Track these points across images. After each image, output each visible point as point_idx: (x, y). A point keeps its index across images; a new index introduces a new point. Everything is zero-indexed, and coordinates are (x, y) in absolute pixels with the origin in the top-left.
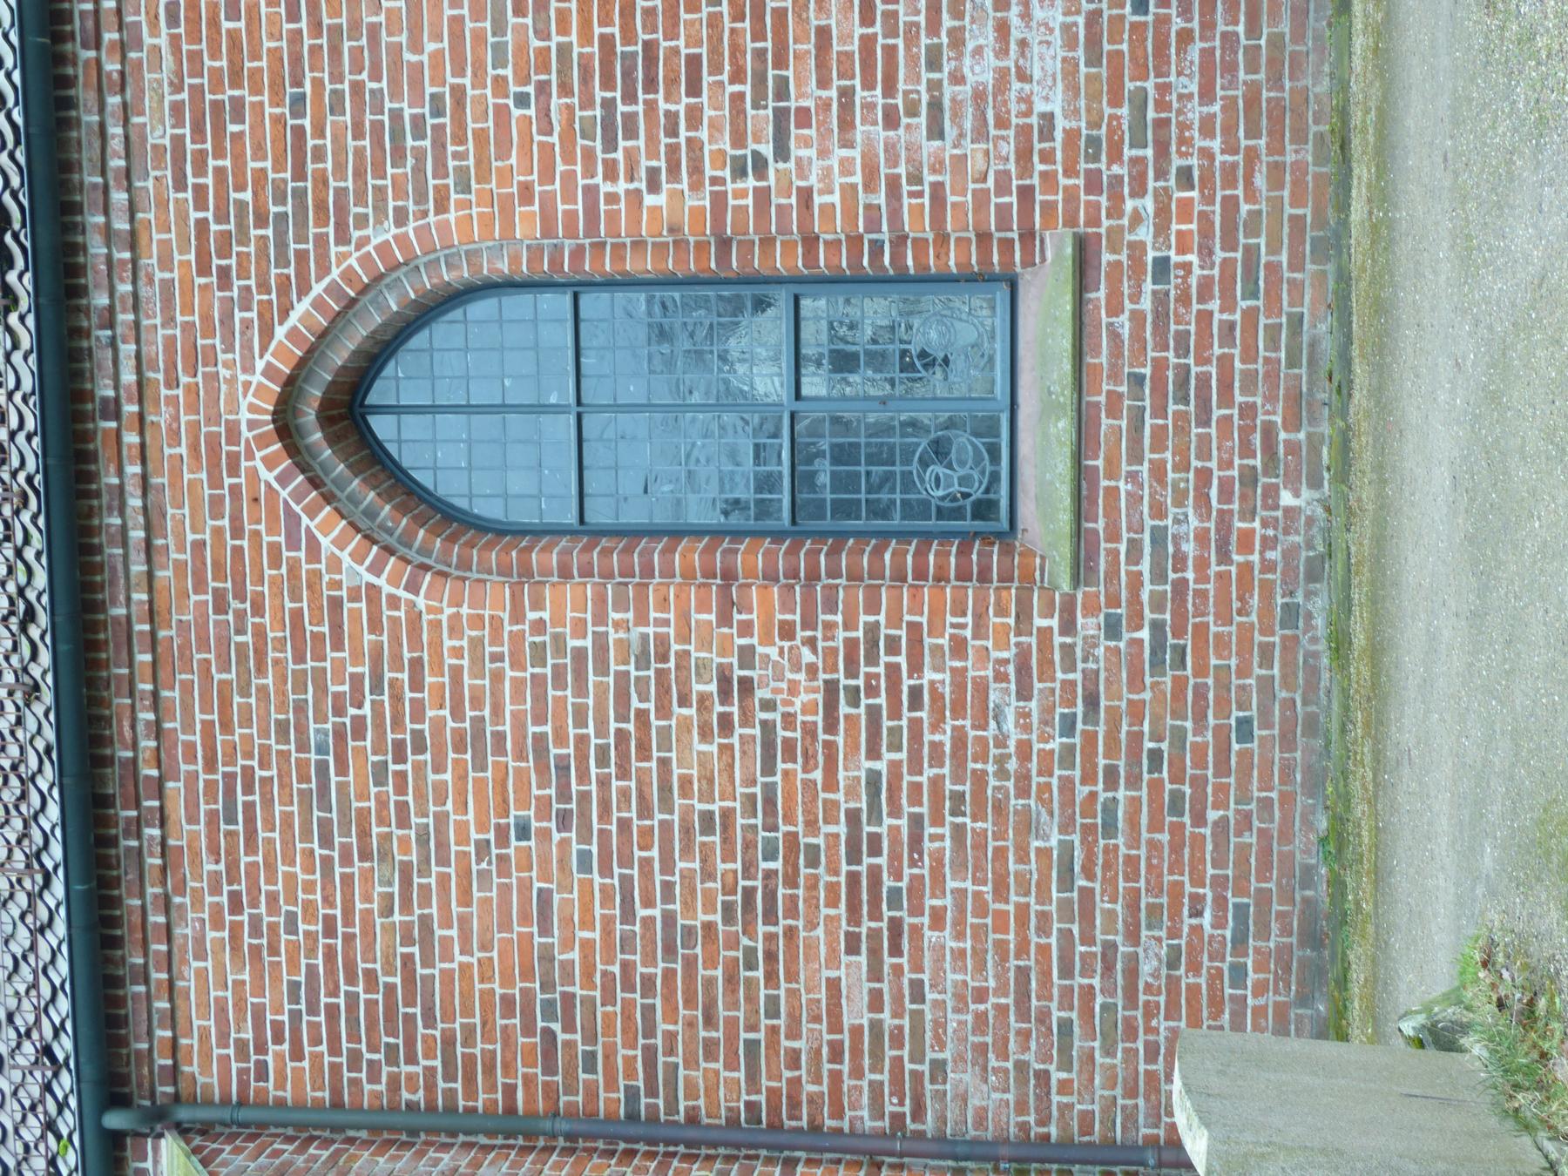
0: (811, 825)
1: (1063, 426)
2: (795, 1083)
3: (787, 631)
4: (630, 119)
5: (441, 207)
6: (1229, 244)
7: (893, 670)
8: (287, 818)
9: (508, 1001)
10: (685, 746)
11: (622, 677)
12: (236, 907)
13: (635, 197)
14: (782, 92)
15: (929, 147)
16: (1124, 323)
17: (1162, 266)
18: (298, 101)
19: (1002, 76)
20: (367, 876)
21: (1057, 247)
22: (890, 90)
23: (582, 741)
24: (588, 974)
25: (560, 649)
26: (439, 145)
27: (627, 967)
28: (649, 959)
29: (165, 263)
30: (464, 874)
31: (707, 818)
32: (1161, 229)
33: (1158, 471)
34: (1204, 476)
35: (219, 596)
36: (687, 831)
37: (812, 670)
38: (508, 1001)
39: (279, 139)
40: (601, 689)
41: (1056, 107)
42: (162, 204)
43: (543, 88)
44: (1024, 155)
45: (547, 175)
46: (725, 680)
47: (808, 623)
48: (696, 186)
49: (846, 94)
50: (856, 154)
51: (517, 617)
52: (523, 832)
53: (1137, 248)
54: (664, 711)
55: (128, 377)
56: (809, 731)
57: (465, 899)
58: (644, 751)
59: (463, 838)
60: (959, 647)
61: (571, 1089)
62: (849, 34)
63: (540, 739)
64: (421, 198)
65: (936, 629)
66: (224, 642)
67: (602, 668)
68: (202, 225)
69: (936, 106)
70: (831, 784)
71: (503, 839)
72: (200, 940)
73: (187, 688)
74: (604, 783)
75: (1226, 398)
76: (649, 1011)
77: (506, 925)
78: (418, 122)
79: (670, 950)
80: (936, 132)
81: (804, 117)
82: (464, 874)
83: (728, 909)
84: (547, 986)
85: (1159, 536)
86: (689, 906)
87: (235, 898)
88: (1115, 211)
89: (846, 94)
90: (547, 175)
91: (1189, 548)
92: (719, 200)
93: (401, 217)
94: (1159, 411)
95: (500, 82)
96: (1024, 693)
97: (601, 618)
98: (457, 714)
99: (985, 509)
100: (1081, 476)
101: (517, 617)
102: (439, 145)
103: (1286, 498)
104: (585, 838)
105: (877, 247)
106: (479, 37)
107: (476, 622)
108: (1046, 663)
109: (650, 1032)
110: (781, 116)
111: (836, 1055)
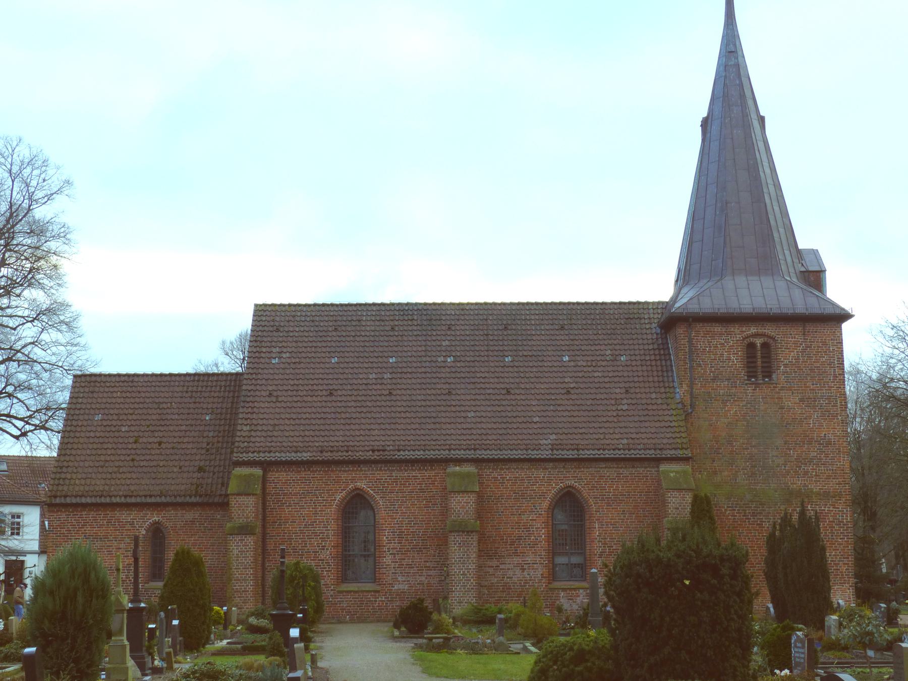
0: (305, 558)
1: (357, 589)
2: (271, 555)
4: (395, 535)
5: (385, 510)
6: (379, 609)
7: (326, 568)
8: (305, 488)
9: (281, 517)
10: (316, 541)
11: (324, 533)
12: (293, 480)
13: (385, 535)
14: (398, 554)
15: (391, 572)
16: (369, 596)
17: (376, 601)
18: (397, 492)
19: (399, 581)
20: (297, 498)
21: (378, 588)
22: (398, 567)
23: (316, 527)
24: (286, 528)
25: (328, 525)
26: (392, 510)
27: (286, 533)
28: (287, 536)
29: (378, 474)
30: (298, 511)
31: (306, 544)
32: (380, 601)
33: (351, 601)
34: (350, 607)
35: (335, 480)
36: (305, 541)
37: (326, 558)
38: (281, 517)
39: (393, 490)
40: (323, 530)
41: (395, 588)
42: (385, 474)
43: (399, 524)
44: (390, 584)
45: (388, 524)
47: (332, 557)
48: (387, 543)
49: (397, 562)
50: (390, 563)
51: (332, 519)
52: (304, 519)
53: (378, 598)
54: (320, 538)
55: (363, 469)
56: (318, 557)
57: (295, 511)
58: (315, 536)
59: (303, 511)
60: (329, 576)
61: (270, 525)
63: (316, 522)
64: (386, 508)
65: (331, 574)
66: (329, 480)
67: (326, 530)
68: (382, 479)
69: (396, 573)
70: (311, 560)
71: (303, 517)
72: (288, 475)
73: (322, 474)
74: (311, 530)
75: (360, 609)
76: (280, 536)
77: (291, 517)
78: (395, 508)
79: (288, 539)
80: (393, 573)
81: (395, 557)
82: (298, 511)
83: (294, 547)
84: (283, 522)
85: (343, 601)
86: (295, 541)
87: (294, 480)
88: (383, 595)
89: (397, 562)
90: (388, 524)
91: (342, 605)
92: (385, 546)
93: (383, 505)
94: (359, 601)
95: (399, 518)
97: (332, 530)
98: (319, 511)
99: (346, 579)
100: (351, 592)
101: (332, 519)
102: (392, 510)
103: (348, 617)
104: (304, 528)
105: (379, 565)
106: (405, 516)
107: (331, 514)
108: (327, 587)
109: (278, 536)
110: (395, 554)
111: (275, 561)
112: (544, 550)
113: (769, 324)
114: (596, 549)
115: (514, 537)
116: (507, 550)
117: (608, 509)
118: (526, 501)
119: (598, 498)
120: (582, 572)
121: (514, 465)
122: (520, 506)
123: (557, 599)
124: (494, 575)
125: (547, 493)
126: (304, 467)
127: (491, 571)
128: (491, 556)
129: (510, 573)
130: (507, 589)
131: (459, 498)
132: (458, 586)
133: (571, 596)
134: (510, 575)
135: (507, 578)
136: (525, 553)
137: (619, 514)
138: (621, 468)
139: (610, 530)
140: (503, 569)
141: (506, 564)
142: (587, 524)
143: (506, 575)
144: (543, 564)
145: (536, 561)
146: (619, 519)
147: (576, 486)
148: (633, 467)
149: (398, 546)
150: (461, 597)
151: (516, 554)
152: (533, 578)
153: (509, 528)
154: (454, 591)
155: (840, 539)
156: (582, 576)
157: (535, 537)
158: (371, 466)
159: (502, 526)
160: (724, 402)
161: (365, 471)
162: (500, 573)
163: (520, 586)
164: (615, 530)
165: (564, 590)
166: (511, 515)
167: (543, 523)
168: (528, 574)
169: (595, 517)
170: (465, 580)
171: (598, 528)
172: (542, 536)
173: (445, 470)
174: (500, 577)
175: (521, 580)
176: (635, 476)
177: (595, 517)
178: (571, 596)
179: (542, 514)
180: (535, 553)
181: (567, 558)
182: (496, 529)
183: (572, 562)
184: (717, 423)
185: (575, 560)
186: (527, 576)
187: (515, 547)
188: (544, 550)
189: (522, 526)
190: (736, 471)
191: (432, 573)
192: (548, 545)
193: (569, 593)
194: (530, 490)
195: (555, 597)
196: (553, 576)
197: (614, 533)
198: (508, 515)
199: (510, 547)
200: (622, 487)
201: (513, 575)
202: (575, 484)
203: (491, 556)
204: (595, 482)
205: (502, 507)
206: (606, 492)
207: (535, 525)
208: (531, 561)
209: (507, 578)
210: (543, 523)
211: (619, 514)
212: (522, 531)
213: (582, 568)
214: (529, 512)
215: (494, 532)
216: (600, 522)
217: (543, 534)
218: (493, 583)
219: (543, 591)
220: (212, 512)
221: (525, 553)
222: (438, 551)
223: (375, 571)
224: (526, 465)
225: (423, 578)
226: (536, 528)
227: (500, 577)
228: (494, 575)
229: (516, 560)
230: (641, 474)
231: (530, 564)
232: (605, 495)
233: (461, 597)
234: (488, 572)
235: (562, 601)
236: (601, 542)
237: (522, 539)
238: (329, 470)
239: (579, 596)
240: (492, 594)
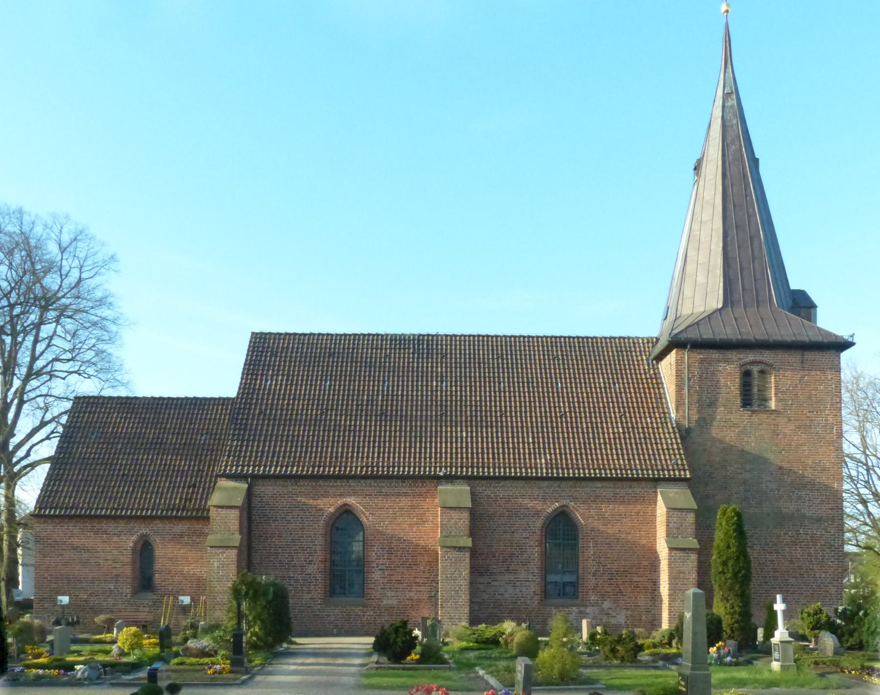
3: (318, 569)
46: (312, 561)
62: (393, 578)
96: (311, 599)
99: (334, 593)
113: (767, 351)
126: (290, 481)
127: (482, 587)
129: (501, 590)
138: (618, 488)
142: (581, 543)
148: (630, 487)
149: (388, 562)
151: (508, 570)
155: (831, 562)
156: (574, 595)
158: (360, 482)
161: (354, 487)
168: (521, 591)
173: (437, 487)
179: (535, 533)
180: (527, 571)
185: (568, 578)
191: (422, 588)
196: (545, 594)
213: (574, 586)
220: (201, 526)
222: (428, 568)
223: (364, 586)
224: (521, 483)
225: (412, 594)
229: (508, 577)
238: (316, 485)
239: (571, 614)
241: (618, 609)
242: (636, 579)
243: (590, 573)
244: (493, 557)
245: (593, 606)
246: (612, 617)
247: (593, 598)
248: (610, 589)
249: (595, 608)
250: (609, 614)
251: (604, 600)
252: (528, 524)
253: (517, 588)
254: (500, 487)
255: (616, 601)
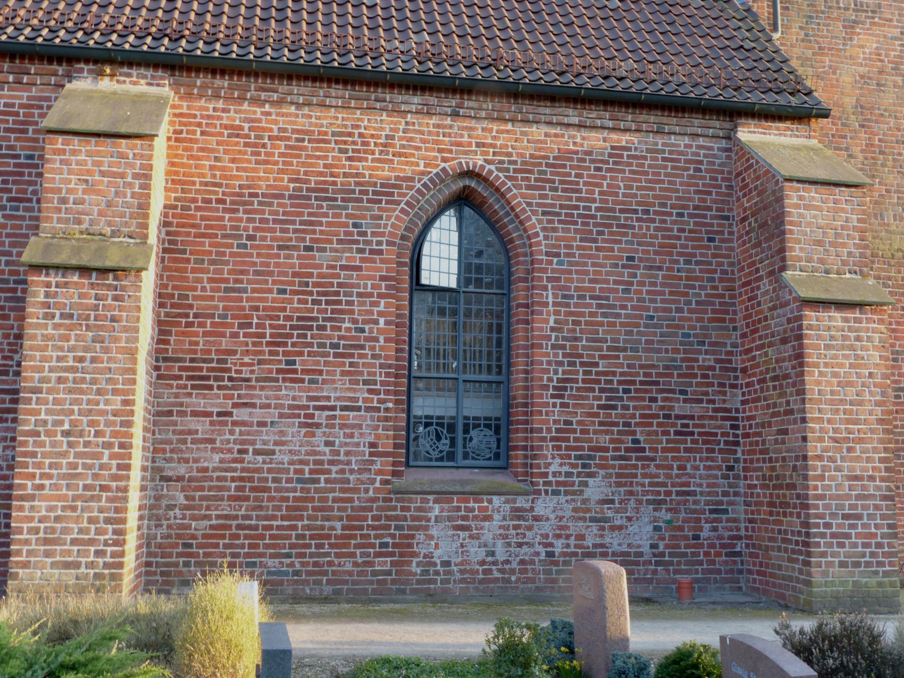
112: (382, 366)
114: (547, 371)
115: (289, 318)
116: (260, 362)
117: (584, 248)
118: (330, 207)
119: (559, 214)
120: (499, 441)
121: (299, 90)
122: (311, 223)
123: (418, 528)
124: (212, 441)
125: (400, 187)
127: (201, 426)
128: (207, 378)
129: (268, 436)
130: (253, 489)
131: (83, 150)
132: (49, 476)
133: (464, 518)
134: (265, 443)
135: (257, 452)
136: (320, 372)
137: (616, 266)
138: (626, 130)
139: (592, 314)
140: (243, 423)
141: (253, 405)
143: (253, 443)
144: (378, 409)
145: (356, 400)
146: (616, 282)
147: (490, 172)
150: (57, 519)
151: (289, 373)
152: (342, 457)
153: (270, 291)
154: (32, 498)
156: (497, 456)
157: (355, 321)
159: (249, 282)
160: (851, 26)
162: (228, 437)
163: (299, 481)
164: (604, 315)
165: (442, 496)
166: (280, 248)
167: (382, 278)
168: (327, 444)
169: (545, 271)
170: (78, 455)
171: (555, 304)
172: (376, 322)
174: (230, 451)
175: (301, 462)
176: (664, 159)
177: (545, 271)
178: (464, 518)
179: (380, 252)
181: (452, 402)
182: (227, 290)
183: (466, 413)
184: (834, 73)
186: (322, 448)
187: (285, 353)
188: (382, 366)
189: (316, 285)
190: (881, 196)
192: (398, 350)
193: (458, 509)
194: (345, 175)
195: (414, 519)
197: (601, 324)
198: (270, 247)
199: (271, 353)
200: (626, 187)
201: (276, 443)
202: (488, 167)
203: (207, 378)
204: (547, 165)
205: (250, 220)
206: (579, 199)
207: (358, 286)
208: (338, 399)
209: (257, 452)
210: (382, 278)
211: (616, 266)
212: (314, 302)
214: (340, 242)
215: (221, 299)
216: (561, 288)
217: (380, 314)
218: (206, 470)
219: (373, 500)
221: (320, 372)
226: (359, 295)
227: (230, 451)
228: (212, 441)
229: (289, 393)
230: (681, 153)
231: (333, 408)
232: (577, 207)
233: (57, 519)
234: (190, 432)
235: (434, 532)
236: (563, 347)
237: (310, 328)
239: (488, 518)
240: (200, 507)
241: (632, 504)
242: (679, 408)
243: (546, 387)
244: (241, 326)
245: (556, 493)
246: (613, 528)
247: (553, 468)
248: (604, 440)
249: (563, 498)
250: (606, 520)
251: (591, 475)
252: (355, 225)
253: (318, 432)
254: (273, 103)
255: (624, 479)
